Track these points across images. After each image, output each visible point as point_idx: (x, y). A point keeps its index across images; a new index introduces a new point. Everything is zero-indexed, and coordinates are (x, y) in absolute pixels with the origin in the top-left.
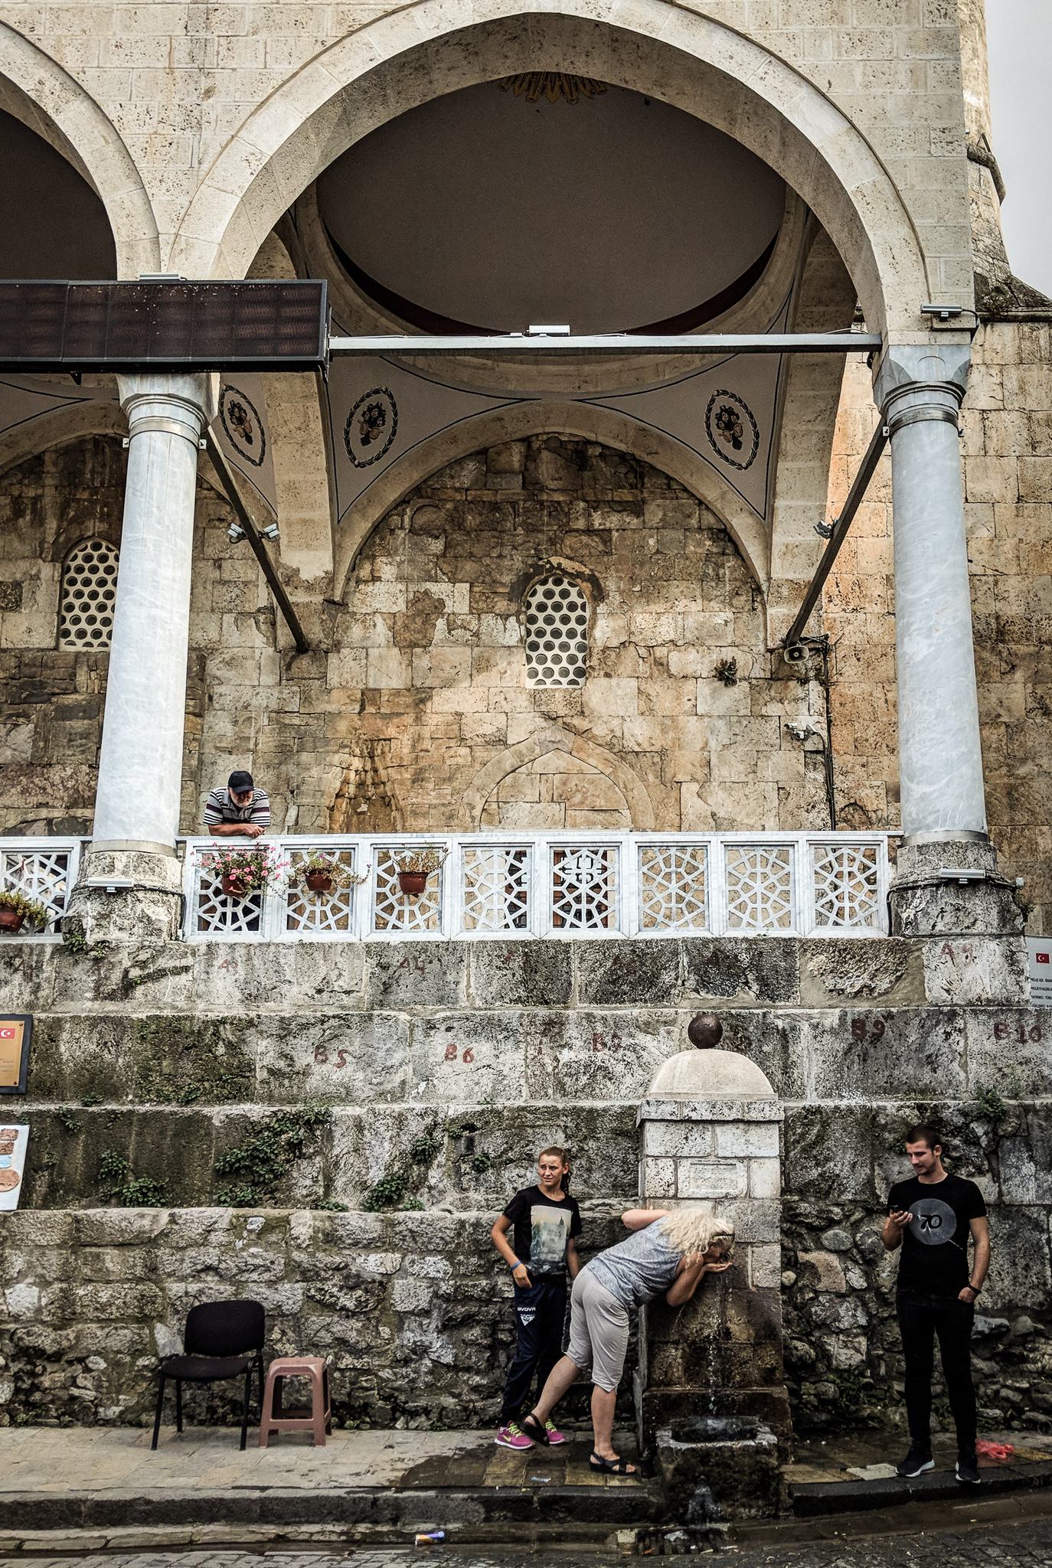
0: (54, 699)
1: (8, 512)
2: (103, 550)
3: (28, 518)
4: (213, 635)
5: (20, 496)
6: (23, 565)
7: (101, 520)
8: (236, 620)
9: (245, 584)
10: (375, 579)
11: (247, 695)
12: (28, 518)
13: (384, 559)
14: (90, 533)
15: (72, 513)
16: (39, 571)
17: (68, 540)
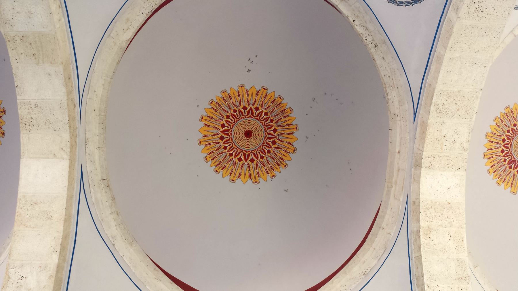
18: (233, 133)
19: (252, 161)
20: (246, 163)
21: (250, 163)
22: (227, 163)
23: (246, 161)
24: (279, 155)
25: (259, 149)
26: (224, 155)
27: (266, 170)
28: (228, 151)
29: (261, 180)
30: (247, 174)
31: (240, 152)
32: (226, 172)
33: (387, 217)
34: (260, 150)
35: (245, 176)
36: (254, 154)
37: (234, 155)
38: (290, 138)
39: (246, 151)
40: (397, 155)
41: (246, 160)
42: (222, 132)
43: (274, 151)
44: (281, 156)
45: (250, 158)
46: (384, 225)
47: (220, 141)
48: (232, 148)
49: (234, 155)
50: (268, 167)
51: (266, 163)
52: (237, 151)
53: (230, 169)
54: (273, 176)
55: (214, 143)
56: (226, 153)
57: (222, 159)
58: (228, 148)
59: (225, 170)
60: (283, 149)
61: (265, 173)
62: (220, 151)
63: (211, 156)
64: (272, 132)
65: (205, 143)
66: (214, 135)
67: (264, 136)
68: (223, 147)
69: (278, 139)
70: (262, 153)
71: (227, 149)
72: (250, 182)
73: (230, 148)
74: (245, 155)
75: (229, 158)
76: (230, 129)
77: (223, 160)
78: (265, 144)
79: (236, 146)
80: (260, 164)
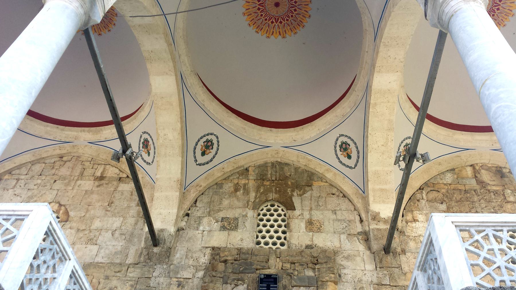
0: (258, 272)
1: (232, 189)
2: (276, 207)
3: (241, 192)
4: (337, 244)
5: (238, 183)
6: (239, 211)
7: (276, 193)
8: (347, 238)
9: (350, 221)
10: (415, 220)
11: (360, 275)
12: (241, 192)
13: (418, 212)
14: (271, 199)
15: (262, 190)
16: (247, 213)
17: (260, 201)
18: (266, 5)
19: (281, 22)
20: (277, 25)
21: (279, 24)
22: (264, 25)
23: (277, 23)
24: (299, 19)
25: (285, 14)
26: (261, 20)
27: (291, 29)
28: (263, 18)
29: (287, 36)
30: (278, 32)
31: (272, 18)
32: (264, 31)
33: (358, 85)
34: (286, 15)
35: (276, 33)
36: (282, 18)
37: (268, 20)
38: (306, 8)
39: (276, 16)
40: (366, 53)
41: (276, 22)
42: (258, 5)
43: (295, 16)
44: (301, 20)
45: (279, 21)
46: (356, 89)
47: (258, 11)
48: (267, 15)
49: (268, 20)
50: (292, 27)
51: (290, 24)
52: (270, 17)
53: (266, 29)
54: (295, 33)
55: (254, 13)
56: (263, 19)
57: (260, 23)
58: (264, 15)
59: (263, 30)
60: (302, 15)
61: (290, 31)
62: (258, 18)
63: (253, 22)
64: (294, 3)
65: (247, 14)
66: (253, 8)
67: (288, 6)
68: (260, 15)
69: (298, 8)
70: (287, 17)
71: (263, 16)
72: (280, 37)
73: (265, 15)
74: (275, 19)
75: (264, 22)
76: (264, 3)
77: (261, 23)
78: (289, 11)
79: (269, 13)
80: (286, 25)
